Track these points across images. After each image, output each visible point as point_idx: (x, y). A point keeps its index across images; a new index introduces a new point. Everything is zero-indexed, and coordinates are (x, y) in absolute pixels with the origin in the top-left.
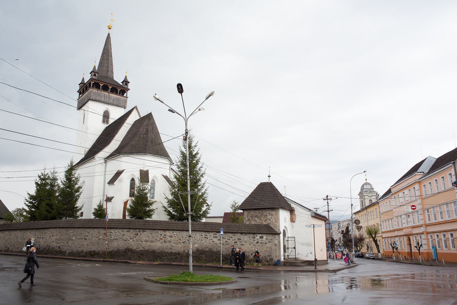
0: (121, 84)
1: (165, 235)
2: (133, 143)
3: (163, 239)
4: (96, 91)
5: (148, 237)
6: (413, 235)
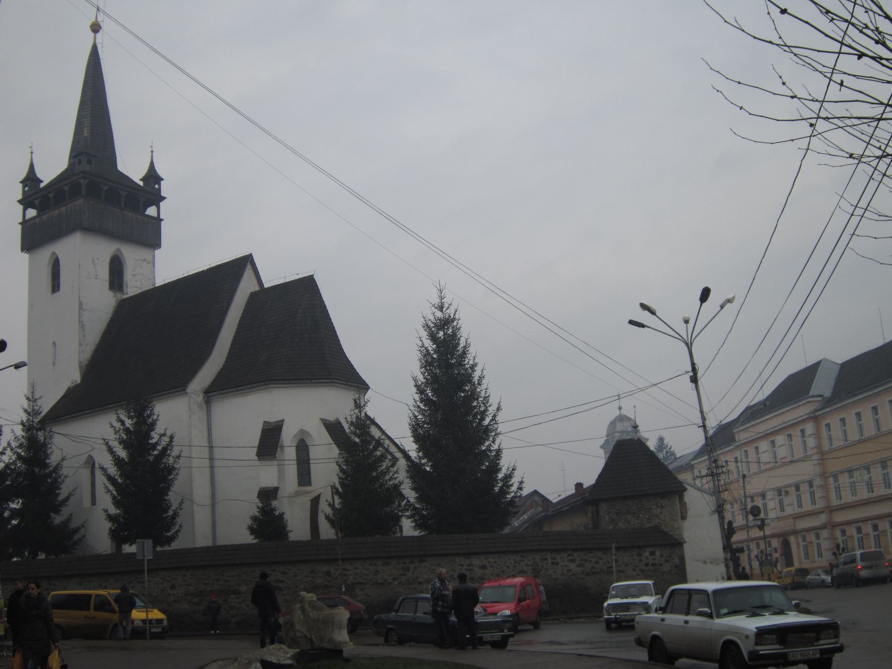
0: (141, 183)
1: (470, 565)
6: (796, 532)
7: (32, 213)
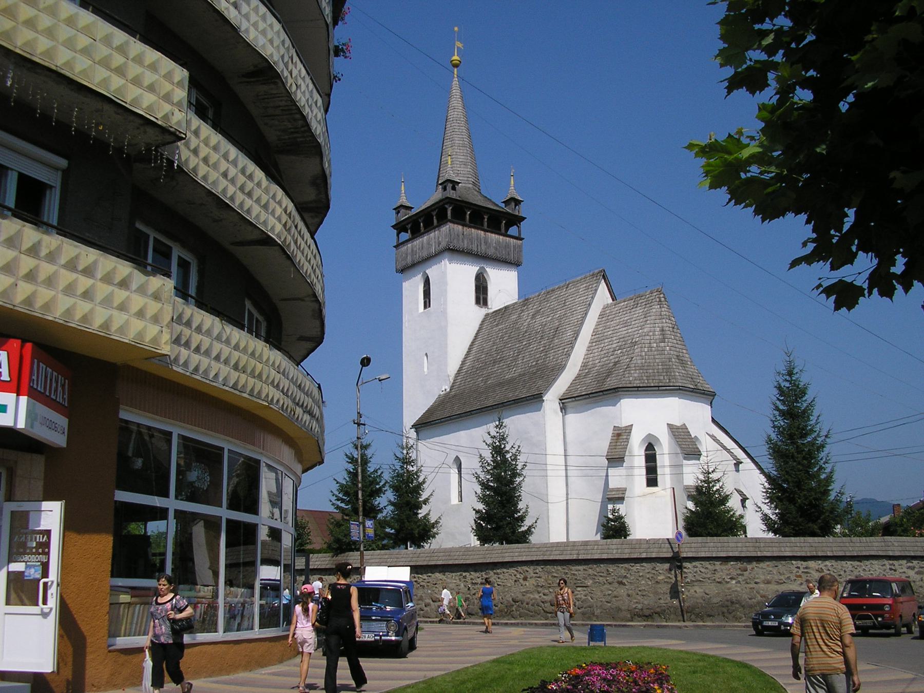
2: (639, 362)
3: (803, 575)
4: (460, 227)
5: (770, 573)
7: (405, 236)
